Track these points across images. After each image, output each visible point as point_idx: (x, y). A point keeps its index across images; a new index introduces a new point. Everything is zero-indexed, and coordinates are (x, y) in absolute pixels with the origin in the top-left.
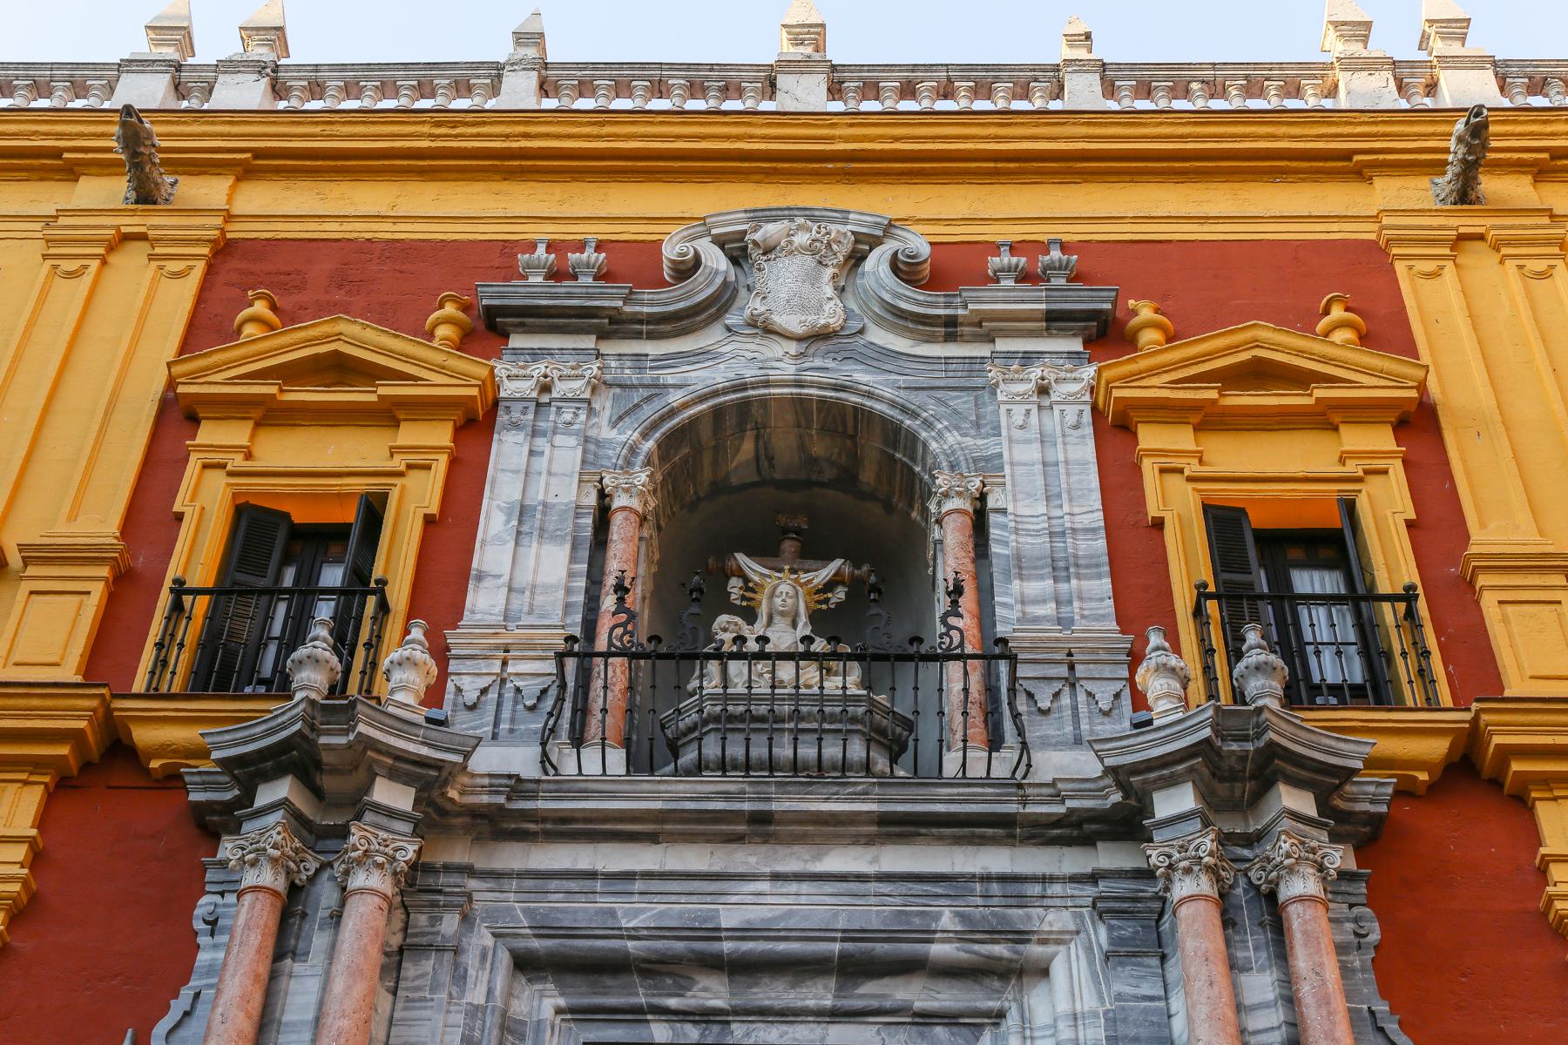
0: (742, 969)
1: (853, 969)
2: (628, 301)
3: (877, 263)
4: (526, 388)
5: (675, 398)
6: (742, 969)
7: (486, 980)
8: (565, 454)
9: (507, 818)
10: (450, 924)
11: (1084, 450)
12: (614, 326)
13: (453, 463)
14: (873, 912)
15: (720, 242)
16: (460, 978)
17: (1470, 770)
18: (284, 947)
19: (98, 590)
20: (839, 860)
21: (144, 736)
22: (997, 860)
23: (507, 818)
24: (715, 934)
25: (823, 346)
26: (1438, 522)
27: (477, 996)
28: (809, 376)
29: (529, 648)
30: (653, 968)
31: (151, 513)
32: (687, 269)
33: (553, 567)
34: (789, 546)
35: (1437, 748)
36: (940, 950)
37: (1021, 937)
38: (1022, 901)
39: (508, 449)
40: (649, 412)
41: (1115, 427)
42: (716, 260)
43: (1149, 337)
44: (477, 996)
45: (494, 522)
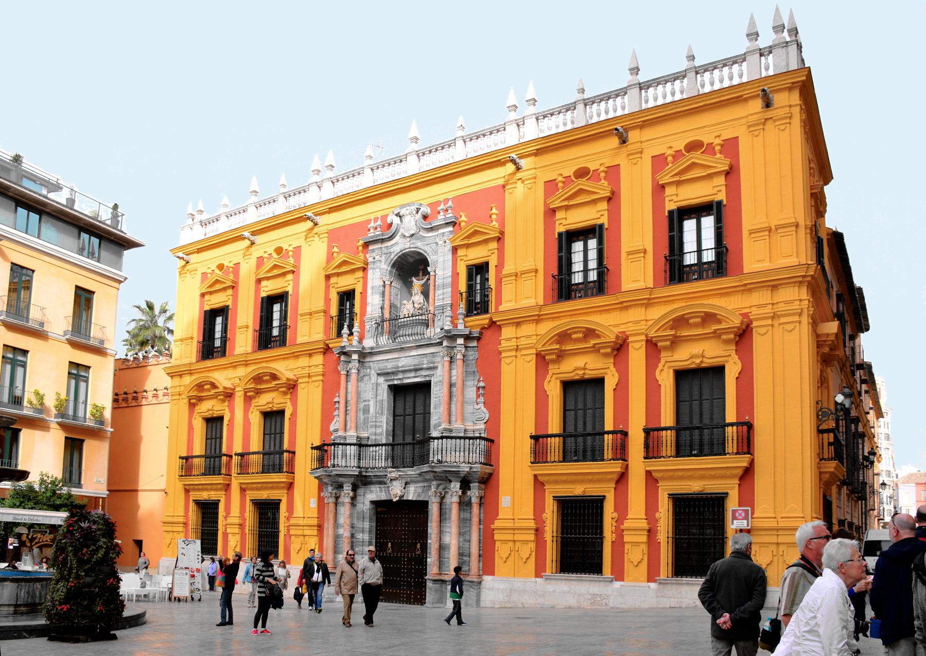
0: (403, 372)
1: (416, 370)
5: (392, 256)
6: (403, 372)
7: (374, 378)
8: (378, 273)
11: (450, 256)
12: (383, 241)
14: (415, 361)
17: (492, 323)
18: (347, 382)
20: (414, 353)
30: (393, 373)
31: (327, 301)
32: (390, 225)
34: (421, 274)
35: (487, 321)
36: (425, 366)
37: (434, 363)
38: (434, 357)
39: (370, 272)
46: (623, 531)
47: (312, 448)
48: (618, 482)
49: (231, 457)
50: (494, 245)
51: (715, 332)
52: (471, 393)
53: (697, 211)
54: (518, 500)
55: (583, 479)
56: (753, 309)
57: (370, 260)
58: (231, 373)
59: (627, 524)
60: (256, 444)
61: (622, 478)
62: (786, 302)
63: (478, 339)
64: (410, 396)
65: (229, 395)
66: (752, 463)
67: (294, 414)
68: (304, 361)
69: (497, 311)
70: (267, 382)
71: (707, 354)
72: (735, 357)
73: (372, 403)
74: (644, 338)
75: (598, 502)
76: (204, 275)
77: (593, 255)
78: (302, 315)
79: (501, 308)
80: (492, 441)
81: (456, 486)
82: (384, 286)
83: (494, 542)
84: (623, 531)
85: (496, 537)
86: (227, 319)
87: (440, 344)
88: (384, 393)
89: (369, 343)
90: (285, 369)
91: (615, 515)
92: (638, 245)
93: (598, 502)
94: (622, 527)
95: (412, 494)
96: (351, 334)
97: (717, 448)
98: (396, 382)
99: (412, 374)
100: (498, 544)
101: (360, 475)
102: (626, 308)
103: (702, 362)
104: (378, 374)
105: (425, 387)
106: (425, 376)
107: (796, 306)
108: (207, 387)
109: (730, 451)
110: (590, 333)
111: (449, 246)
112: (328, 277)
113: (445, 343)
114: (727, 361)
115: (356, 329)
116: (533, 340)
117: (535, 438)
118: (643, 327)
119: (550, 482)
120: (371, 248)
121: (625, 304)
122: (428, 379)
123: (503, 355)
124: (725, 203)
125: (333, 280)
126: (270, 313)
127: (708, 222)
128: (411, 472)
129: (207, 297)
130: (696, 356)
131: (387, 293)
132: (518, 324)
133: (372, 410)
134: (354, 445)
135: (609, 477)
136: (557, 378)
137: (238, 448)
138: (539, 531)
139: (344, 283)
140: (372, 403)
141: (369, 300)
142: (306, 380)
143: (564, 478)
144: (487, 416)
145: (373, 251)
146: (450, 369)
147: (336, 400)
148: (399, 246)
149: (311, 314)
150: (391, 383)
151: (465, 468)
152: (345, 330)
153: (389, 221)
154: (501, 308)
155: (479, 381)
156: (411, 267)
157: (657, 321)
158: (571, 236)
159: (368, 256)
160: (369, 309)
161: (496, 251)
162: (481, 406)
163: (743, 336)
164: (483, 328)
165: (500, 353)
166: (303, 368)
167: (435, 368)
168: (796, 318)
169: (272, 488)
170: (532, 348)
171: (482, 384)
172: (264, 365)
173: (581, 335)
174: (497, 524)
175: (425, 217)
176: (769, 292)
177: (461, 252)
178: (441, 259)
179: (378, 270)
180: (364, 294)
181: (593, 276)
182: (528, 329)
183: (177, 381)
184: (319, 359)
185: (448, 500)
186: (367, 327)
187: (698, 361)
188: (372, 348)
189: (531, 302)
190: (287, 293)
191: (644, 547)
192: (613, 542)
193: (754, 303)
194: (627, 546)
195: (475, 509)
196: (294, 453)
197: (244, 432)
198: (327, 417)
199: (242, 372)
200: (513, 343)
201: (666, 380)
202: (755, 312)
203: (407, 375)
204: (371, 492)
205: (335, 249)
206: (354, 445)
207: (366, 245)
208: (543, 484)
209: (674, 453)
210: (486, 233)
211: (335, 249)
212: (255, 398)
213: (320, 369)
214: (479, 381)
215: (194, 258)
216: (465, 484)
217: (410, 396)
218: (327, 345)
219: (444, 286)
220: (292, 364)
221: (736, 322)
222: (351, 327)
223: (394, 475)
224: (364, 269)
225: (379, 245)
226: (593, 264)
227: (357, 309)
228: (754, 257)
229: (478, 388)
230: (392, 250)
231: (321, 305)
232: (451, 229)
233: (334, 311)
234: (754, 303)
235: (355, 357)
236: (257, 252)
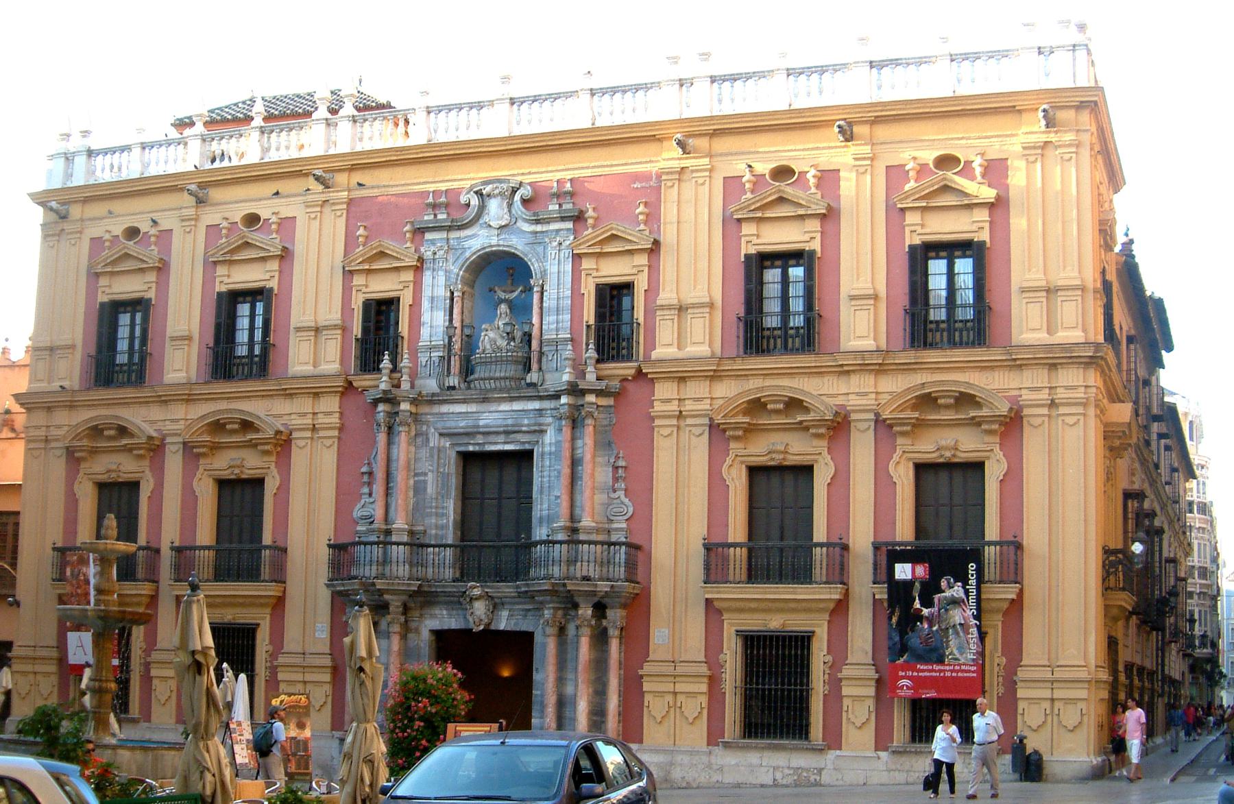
1: (507, 433)
2: (455, 215)
3: (517, 197)
4: (429, 253)
5: (468, 254)
7: (434, 440)
8: (441, 279)
9: (433, 400)
10: (424, 428)
11: (569, 267)
12: (449, 229)
13: (415, 283)
15: (476, 193)
16: (428, 440)
17: (640, 374)
18: (390, 443)
19: (339, 337)
20: (505, 407)
21: (355, 384)
22: (536, 405)
23: (433, 400)
24: (478, 426)
25: (505, 230)
26: (652, 291)
27: (432, 445)
28: (501, 243)
29: (435, 347)
30: (467, 434)
33: (440, 318)
35: (632, 372)
36: (524, 429)
37: (540, 425)
39: (427, 277)
40: (460, 261)
41: (577, 257)
42: (475, 201)
43: (590, 221)
44: (432, 445)
45: (426, 304)
46: (841, 680)
47: (330, 546)
48: (833, 612)
49: (158, 551)
50: (642, 260)
51: (973, 418)
52: (604, 475)
53: (951, 249)
54: (685, 634)
55: (781, 607)
56: (1023, 392)
57: (428, 255)
58: (156, 413)
59: (846, 672)
60: (205, 534)
61: (840, 609)
62: (1066, 388)
63: (617, 395)
64: (495, 475)
65: (156, 449)
66: (1021, 594)
67: (284, 488)
68: (305, 404)
69: (647, 359)
70: (233, 432)
71: (962, 447)
72: (1000, 454)
73: (430, 477)
74: (872, 416)
75: (803, 641)
76: (96, 242)
77: (796, 290)
78: (298, 329)
79: (655, 355)
80: (638, 548)
81: (586, 611)
82: (452, 299)
83: (642, 694)
84: (841, 680)
85: (646, 687)
86: (145, 320)
87: (557, 396)
88: (451, 466)
89: (430, 385)
90: (270, 412)
91: (829, 658)
92: (863, 285)
93: (803, 641)
94: (840, 675)
95: (503, 622)
96: (395, 369)
97: (801, 573)
98: (471, 448)
99: (501, 438)
100: (647, 698)
101: (419, 592)
102: (848, 372)
103: (954, 456)
104: (441, 435)
105: (524, 458)
106: (524, 443)
107: (1080, 394)
108: (112, 432)
109: (818, 579)
110: (794, 404)
111: (566, 253)
112: (348, 274)
113: (564, 400)
114: (988, 458)
115: (405, 362)
116: (704, 405)
117: (708, 548)
118: (869, 401)
119: (729, 610)
120: (428, 236)
121: (846, 368)
122: (527, 447)
123: (657, 422)
124: (988, 245)
125: (358, 280)
126: (232, 317)
127: (964, 266)
128: (506, 589)
129: (103, 281)
130: (947, 448)
131: (456, 311)
132: (682, 380)
133: (431, 490)
134: (405, 544)
135: (821, 606)
136: (742, 462)
137: (170, 535)
138: (714, 681)
139: (381, 287)
140: (430, 477)
141: (426, 317)
142: (309, 434)
143: (753, 605)
144: (631, 510)
145: (433, 242)
146: (573, 439)
147: (364, 469)
148: (478, 240)
149: (317, 330)
150: (462, 449)
151: (604, 587)
152: (386, 363)
153: (463, 199)
154: (655, 355)
155: (617, 458)
156: (502, 274)
157: (900, 395)
158: (764, 260)
159: (422, 250)
160: (425, 332)
161: (646, 269)
162: (621, 494)
163: (1011, 425)
164: (624, 380)
165: (653, 419)
166: (305, 414)
167: (542, 432)
168: (1080, 410)
169: (242, 605)
170: (704, 416)
171: (621, 463)
172: (223, 405)
173: (781, 406)
174: (647, 668)
175: (525, 202)
176: (1046, 371)
177: (587, 264)
178: (552, 269)
179: (441, 273)
180: (416, 306)
181: (797, 321)
182: (695, 389)
183: (40, 418)
184: (331, 404)
185: (571, 630)
186: (423, 359)
187: (948, 454)
188: (433, 395)
189: (703, 350)
190: (271, 289)
191: (871, 703)
192: (825, 695)
193: (1026, 386)
194: (846, 702)
195: (614, 645)
196: (285, 550)
197: (181, 510)
198: (344, 499)
199: (179, 411)
200: (674, 407)
201: (904, 478)
202: (1026, 396)
203: (492, 438)
204: (433, 616)
205: (361, 231)
206: (405, 544)
207: (420, 231)
208: (720, 612)
209: (744, 577)
210: (630, 241)
211: (361, 231)
212: (204, 455)
213: (335, 419)
214: (617, 458)
215: (76, 211)
216: (600, 609)
217: (495, 475)
218: (350, 383)
219: (558, 311)
220: (281, 407)
221: (1003, 408)
222: (394, 361)
223: (477, 592)
224: (419, 269)
225: (444, 235)
226: (797, 305)
227: (404, 328)
228: (1027, 324)
229: (616, 468)
230: (466, 244)
231: (335, 316)
232: (570, 225)
233: (357, 330)
234: (1026, 386)
235: (405, 406)
236: (211, 217)
